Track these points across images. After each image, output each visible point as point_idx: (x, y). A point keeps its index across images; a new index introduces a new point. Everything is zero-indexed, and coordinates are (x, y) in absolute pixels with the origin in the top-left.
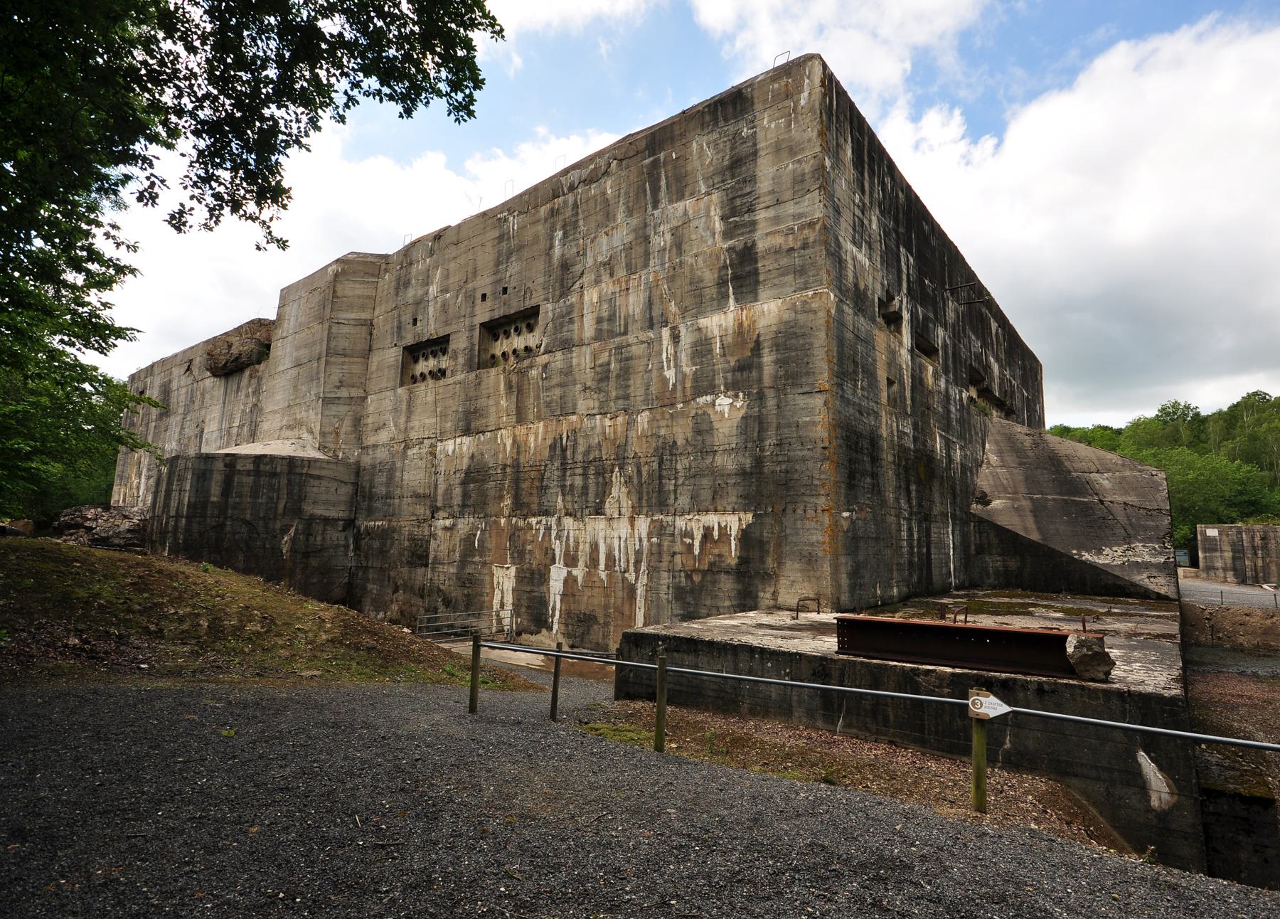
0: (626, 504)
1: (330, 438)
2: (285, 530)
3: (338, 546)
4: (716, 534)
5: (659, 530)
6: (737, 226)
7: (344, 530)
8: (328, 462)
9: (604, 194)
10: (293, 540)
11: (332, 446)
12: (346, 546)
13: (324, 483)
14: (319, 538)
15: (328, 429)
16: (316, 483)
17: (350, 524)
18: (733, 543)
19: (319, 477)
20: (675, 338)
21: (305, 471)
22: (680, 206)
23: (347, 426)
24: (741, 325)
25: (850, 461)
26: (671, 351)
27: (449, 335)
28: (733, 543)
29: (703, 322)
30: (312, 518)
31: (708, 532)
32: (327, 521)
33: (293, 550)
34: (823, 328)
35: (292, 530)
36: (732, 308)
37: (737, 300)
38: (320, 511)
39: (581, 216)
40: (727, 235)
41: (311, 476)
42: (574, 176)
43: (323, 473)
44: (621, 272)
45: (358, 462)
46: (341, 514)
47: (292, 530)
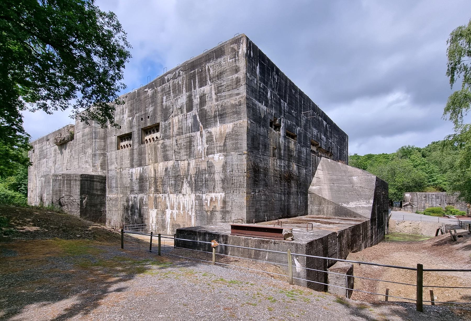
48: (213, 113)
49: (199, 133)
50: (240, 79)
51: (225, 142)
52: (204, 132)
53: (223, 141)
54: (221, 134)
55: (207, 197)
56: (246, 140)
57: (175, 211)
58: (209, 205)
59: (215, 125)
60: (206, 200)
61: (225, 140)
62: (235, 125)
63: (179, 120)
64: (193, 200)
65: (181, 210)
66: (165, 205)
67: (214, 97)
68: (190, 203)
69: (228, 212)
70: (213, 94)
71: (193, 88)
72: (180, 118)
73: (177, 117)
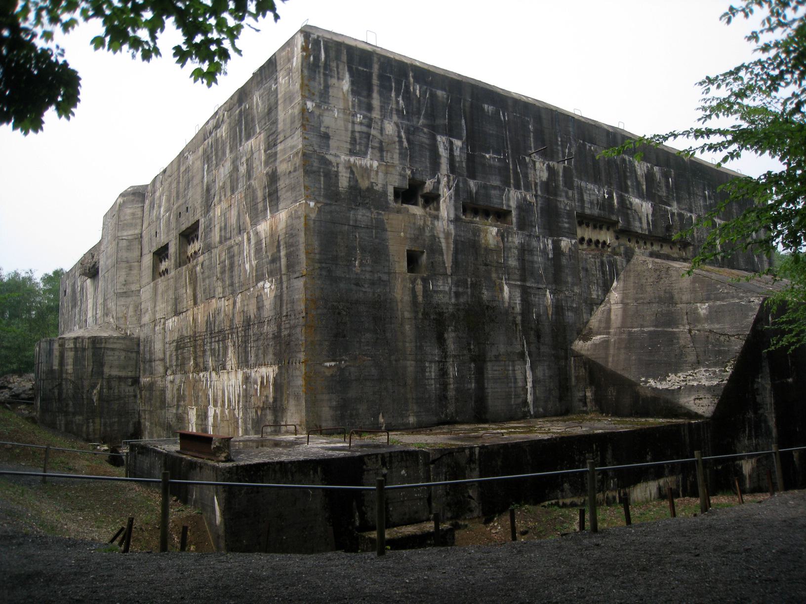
0: (234, 361)
1: (122, 321)
2: (93, 387)
3: (129, 396)
5: (247, 379)
7: (132, 385)
8: (118, 338)
10: (100, 393)
11: (123, 326)
12: (135, 396)
13: (117, 353)
14: (116, 391)
15: (120, 315)
16: (109, 353)
17: (136, 381)
19: (113, 349)
20: (249, 239)
21: (103, 345)
22: (249, 142)
23: (131, 312)
27: (168, 244)
30: (110, 378)
31: (262, 378)
32: (120, 378)
33: (100, 399)
34: (303, 229)
35: (98, 387)
38: (115, 372)
40: (267, 163)
41: (108, 349)
42: (211, 125)
43: (115, 346)
45: (139, 339)
46: (130, 374)
47: (98, 387)
52: (252, 234)
54: (272, 235)
66: (207, 396)
67: (263, 158)
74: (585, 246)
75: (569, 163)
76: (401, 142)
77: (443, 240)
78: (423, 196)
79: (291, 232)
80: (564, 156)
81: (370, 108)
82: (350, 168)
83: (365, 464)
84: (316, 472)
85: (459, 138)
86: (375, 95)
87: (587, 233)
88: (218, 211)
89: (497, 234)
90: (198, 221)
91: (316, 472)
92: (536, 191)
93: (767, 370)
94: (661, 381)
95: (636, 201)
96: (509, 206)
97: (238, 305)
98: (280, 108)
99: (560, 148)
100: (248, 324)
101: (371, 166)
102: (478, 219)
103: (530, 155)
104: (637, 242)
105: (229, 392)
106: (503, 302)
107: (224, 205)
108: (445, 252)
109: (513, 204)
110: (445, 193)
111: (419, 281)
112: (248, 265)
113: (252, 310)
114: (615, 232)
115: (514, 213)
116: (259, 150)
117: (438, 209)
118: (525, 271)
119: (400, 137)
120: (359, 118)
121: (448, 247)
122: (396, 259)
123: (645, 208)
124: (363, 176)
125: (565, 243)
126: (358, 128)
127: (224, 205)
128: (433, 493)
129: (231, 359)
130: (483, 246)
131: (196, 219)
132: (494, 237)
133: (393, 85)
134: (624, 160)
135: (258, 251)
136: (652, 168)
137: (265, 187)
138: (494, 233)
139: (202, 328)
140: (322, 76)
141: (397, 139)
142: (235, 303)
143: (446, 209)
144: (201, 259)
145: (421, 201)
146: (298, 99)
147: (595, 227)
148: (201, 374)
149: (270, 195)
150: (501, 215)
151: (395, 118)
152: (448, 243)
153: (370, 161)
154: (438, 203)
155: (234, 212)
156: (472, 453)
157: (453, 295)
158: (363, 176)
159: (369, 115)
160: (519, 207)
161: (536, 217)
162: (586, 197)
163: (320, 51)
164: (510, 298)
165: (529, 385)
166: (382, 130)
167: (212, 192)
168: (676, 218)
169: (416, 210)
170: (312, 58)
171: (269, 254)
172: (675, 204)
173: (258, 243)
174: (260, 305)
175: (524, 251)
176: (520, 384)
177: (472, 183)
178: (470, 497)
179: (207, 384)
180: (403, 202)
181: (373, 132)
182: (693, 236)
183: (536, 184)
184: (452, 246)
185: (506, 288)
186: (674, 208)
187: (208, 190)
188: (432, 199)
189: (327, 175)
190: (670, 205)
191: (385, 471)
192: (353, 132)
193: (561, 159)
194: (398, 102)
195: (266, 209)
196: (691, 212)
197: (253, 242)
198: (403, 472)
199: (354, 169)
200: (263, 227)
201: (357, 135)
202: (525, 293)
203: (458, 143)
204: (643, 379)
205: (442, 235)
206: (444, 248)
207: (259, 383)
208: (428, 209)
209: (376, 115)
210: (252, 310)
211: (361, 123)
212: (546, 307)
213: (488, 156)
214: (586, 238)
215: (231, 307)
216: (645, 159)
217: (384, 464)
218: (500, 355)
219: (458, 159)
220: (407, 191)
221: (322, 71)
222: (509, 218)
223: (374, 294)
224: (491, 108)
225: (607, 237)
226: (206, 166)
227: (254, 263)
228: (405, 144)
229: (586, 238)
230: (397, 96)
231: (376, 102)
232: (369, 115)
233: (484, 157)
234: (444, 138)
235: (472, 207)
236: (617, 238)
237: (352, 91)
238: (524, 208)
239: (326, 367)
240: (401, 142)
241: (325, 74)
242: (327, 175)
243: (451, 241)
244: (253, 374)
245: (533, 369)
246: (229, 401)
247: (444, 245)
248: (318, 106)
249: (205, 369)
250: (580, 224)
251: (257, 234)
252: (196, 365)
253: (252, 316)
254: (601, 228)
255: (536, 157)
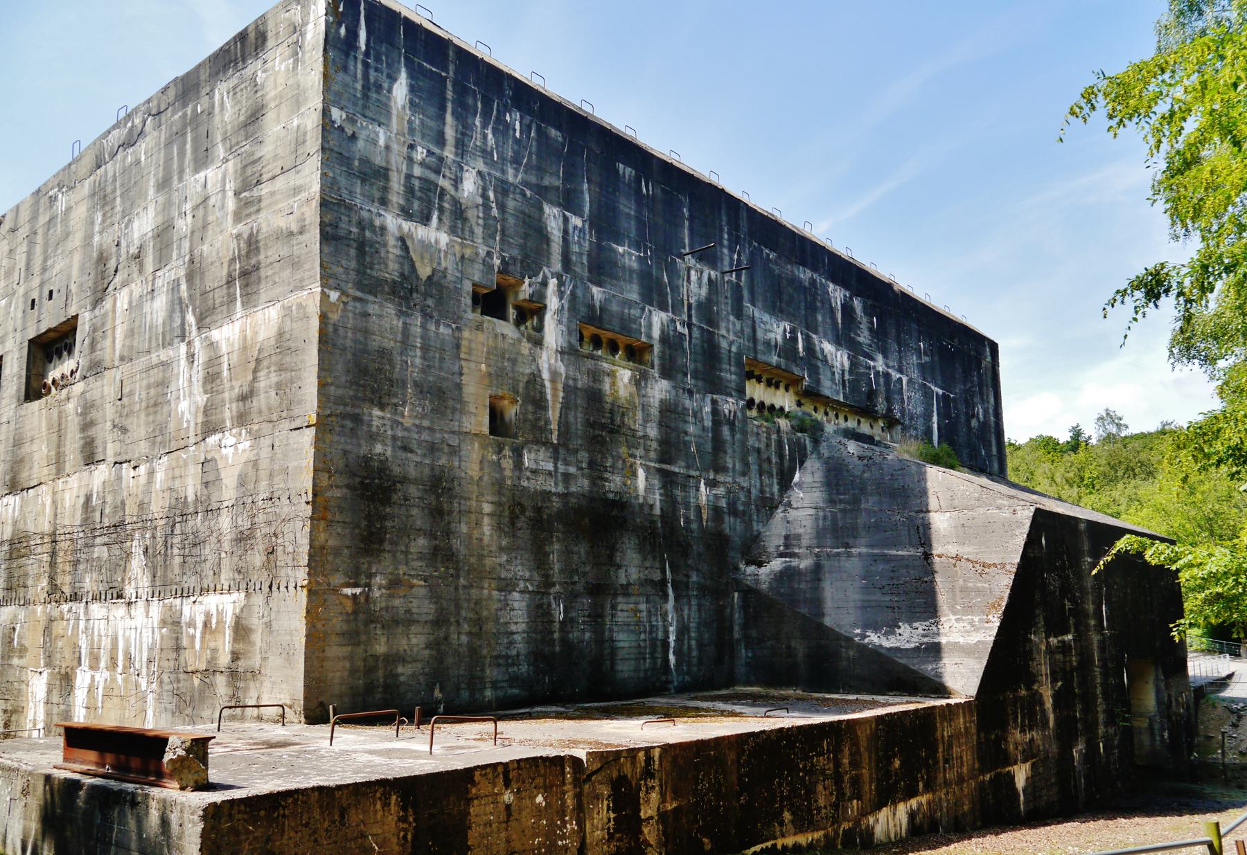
4: (214, 621)
6: (248, 203)
9: (138, 162)
18: (227, 632)
20: (191, 357)
24: (245, 338)
25: (368, 517)
26: (187, 375)
28: (227, 632)
29: (215, 335)
36: (239, 315)
37: (243, 304)
39: (118, 192)
40: (238, 217)
42: (117, 136)
44: (149, 267)
48: (226, 265)
49: (183, 348)
50: (305, 134)
51: (255, 379)
52: (197, 344)
53: (250, 377)
54: (244, 348)
55: (193, 610)
56: (316, 369)
57: (102, 676)
58: (198, 646)
59: (229, 316)
60: (192, 624)
61: (255, 371)
62: (287, 312)
63: (130, 303)
64: (156, 625)
65: (120, 669)
66: (76, 648)
67: (231, 204)
68: (147, 639)
69: (254, 674)
70: (230, 194)
71: (176, 178)
72: (136, 294)
73: (125, 291)
74: (754, 413)
75: (739, 277)
76: (486, 207)
77: (548, 384)
78: (517, 307)
79: (283, 342)
80: (731, 265)
81: (441, 140)
82: (402, 239)
83: (474, 783)
84: (386, 805)
85: (579, 213)
86: (449, 118)
87: (756, 391)
88: (123, 300)
89: (630, 380)
90: (76, 317)
91: (386, 805)
92: (690, 316)
93: (1041, 622)
94: (886, 634)
95: (828, 348)
96: (649, 336)
97: (160, 476)
98: (270, 116)
99: (726, 251)
100: (179, 512)
101: (437, 241)
102: (600, 353)
103: (682, 256)
104: (826, 414)
105: (127, 641)
106: (637, 497)
107: (137, 288)
108: (550, 403)
109: (656, 333)
110: (553, 302)
111: (507, 451)
112: (187, 405)
113: (191, 488)
114: (797, 394)
115: (656, 349)
116: (223, 191)
117: (540, 328)
118: (670, 447)
119: (484, 196)
120: (420, 154)
121: (555, 395)
122: (472, 409)
123: (839, 358)
124: (422, 258)
125: (729, 405)
126: (417, 171)
127: (137, 288)
128: (588, 841)
129: (138, 576)
130: (609, 399)
131: (72, 312)
132: (625, 386)
133: (479, 105)
134: (815, 281)
135: (211, 378)
136: (851, 298)
137: (233, 260)
138: (626, 380)
139: (71, 517)
140: (360, 66)
141: (480, 201)
142: (151, 473)
143: (553, 334)
144: (78, 388)
145: (512, 313)
146: (315, 101)
147: (769, 384)
148: (65, 607)
149: (245, 274)
150: (636, 354)
151: (481, 165)
152: (555, 389)
153: (434, 234)
154: (541, 320)
155: (160, 304)
156: (649, 759)
157: (560, 478)
158: (422, 258)
159: (437, 151)
160: (664, 339)
161: (687, 360)
162: (760, 334)
163: (358, 20)
164: (646, 489)
165: (672, 638)
166: (457, 182)
167: (112, 264)
168: (882, 380)
169: (507, 328)
170: (343, 31)
171: (236, 384)
172: (880, 357)
173: (213, 361)
174: (211, 478)
175: (670, 413)
176: (660, 635)
177: (595, 290)
178: (646, 841)
179: (76, 627)
180: (482, 313)
181: (444, 183)
182: (902, 411)
183: (690, 306)
184: (561, 394)
185: (641, 473)
186: (879, 364)
187: (102, 259)
188: (531, 313)
189: (362, 246)
190: (873, 359)
191: (508, 797)
192: (409, 177)
193: (727, 269)
194: (485, 137)
195: (231, 300)
196: (901, 372)
197: (201, 358)
198: (539, 799)
199: (409, 243)
200: (226, 335)
201: (417, 183)
202: (668, 480)
203: (576, 221)
204: (858, 631)
205: (546, 375)
206: (549, 397)
207: (200, 625)
208: (522, 328)
209: (449, 153)
210: (191, 488)
211: (423, 164)
212: (699, 509)
213: (621, 249)
214: (757, 401)
215: (143, 480)
216: (843, 283)
217: (507, 784)
218: (629, 584)
219: (576, 248)
220: (493, 292)
221: (360, 57)
222: (647, 357)
223: (432, 469)
224: (628, 170)
225: (784, 400)
226: (99, 218)
227: (201, 399)
228: (495, 212)
229: (757, 401)
230: (484, 126)
231: (450, 133)
232: (437, 151)
233: (615, 251)
234: (556, 211)
235: (597, 333)
236: (799, 404)
237: (411, 103)
238: (670, 341)
239: (346, 596)
240: (486, 207)
241: (366, 65)
242: (362, 246)
243: (560, 386)
244: (186, 610)
245: (678, 609)
246: (129, 659)
247: (549, 391)
248: (351, 120)
249: (75, 597)
250: (750, 376)
251: (212, 345)
252: (54, 587)
253: (191, 498)
254: (777, 387)
255: (691, 261)
